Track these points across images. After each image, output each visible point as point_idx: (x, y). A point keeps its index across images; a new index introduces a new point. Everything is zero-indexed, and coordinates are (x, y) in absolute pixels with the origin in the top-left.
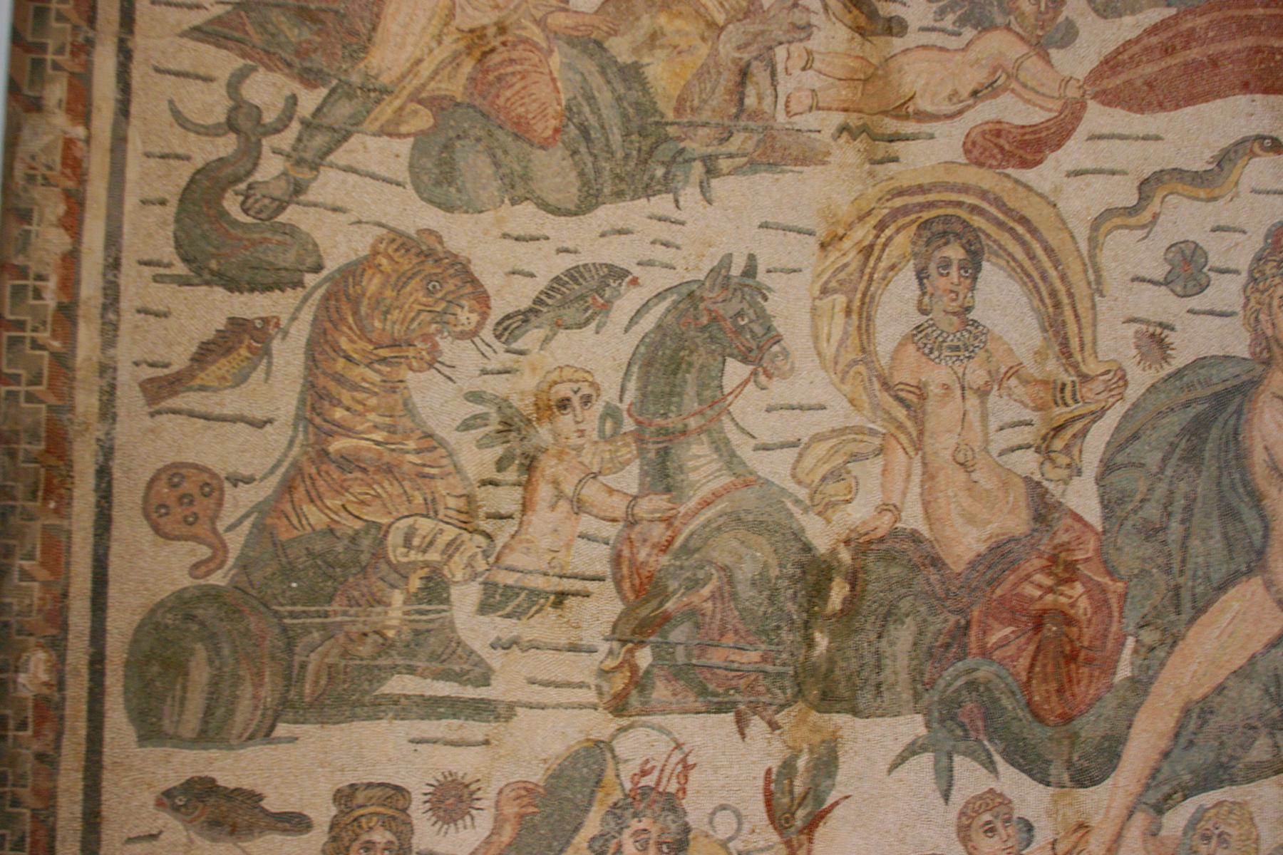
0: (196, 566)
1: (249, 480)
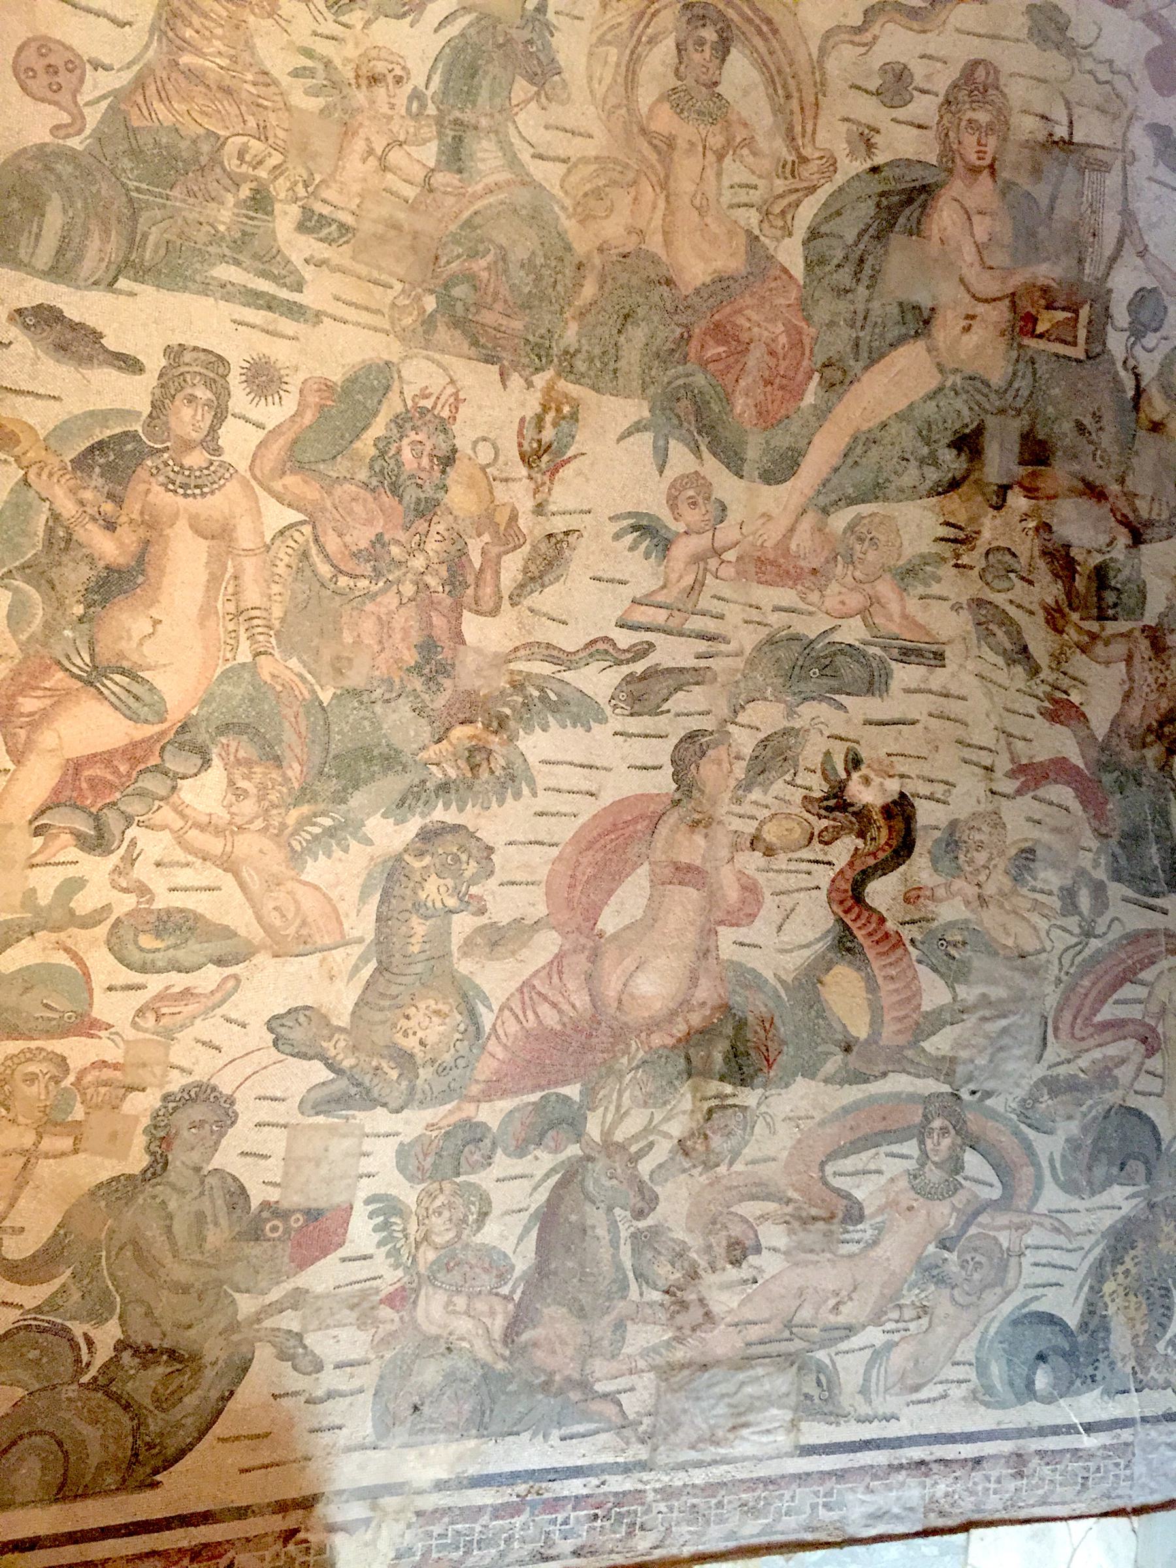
0: (57, 127)
1: (107, 68)
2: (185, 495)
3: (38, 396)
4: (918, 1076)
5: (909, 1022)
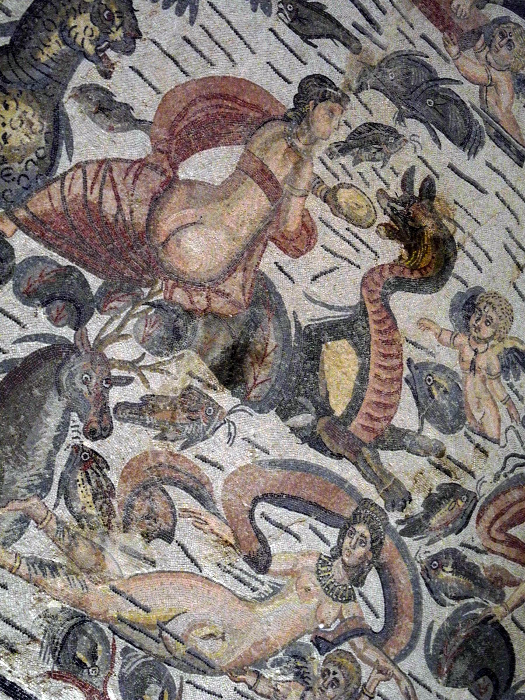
4: (364, 476)
5: (378, 426)
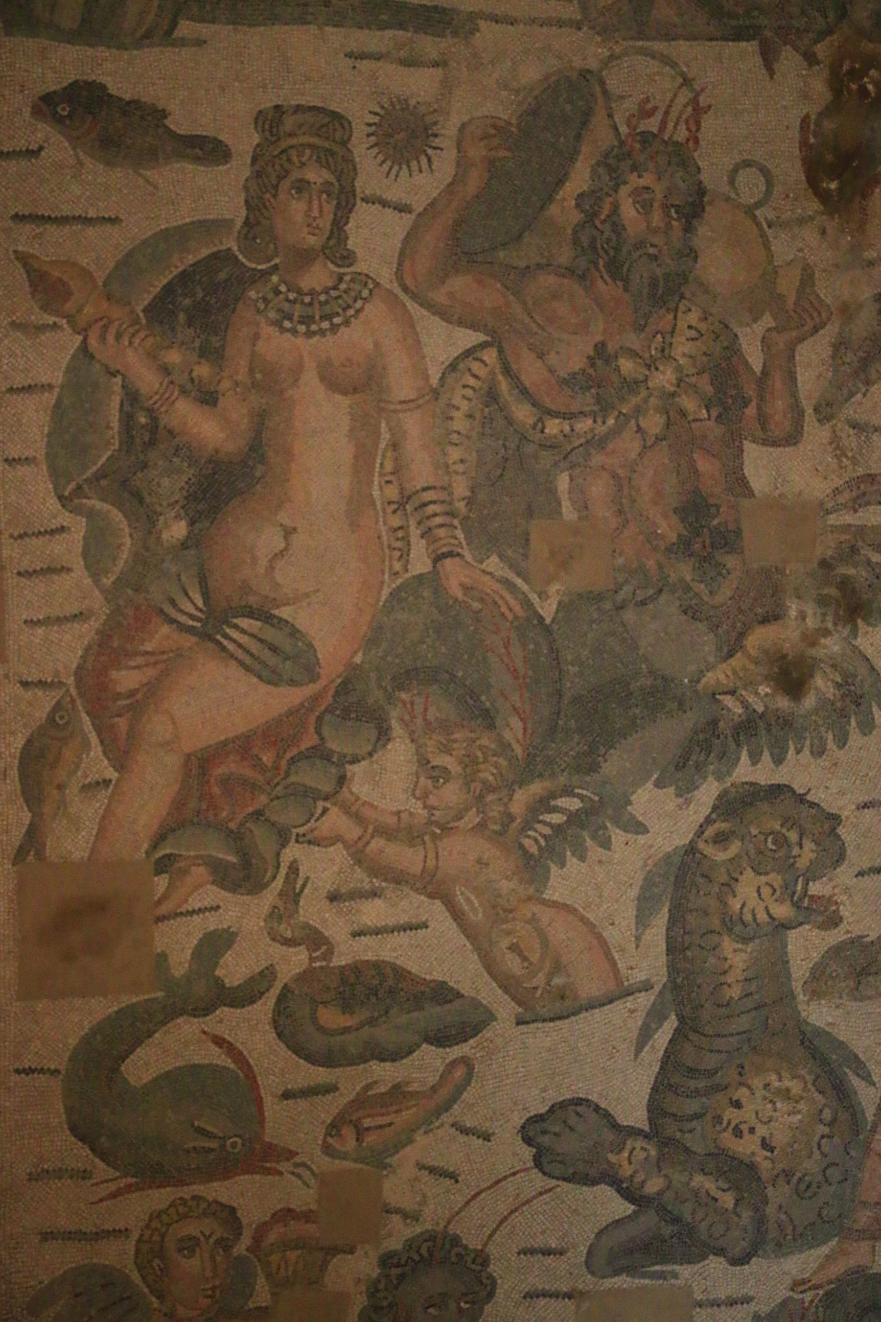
2: (309, 334)
3: (87, 221)
